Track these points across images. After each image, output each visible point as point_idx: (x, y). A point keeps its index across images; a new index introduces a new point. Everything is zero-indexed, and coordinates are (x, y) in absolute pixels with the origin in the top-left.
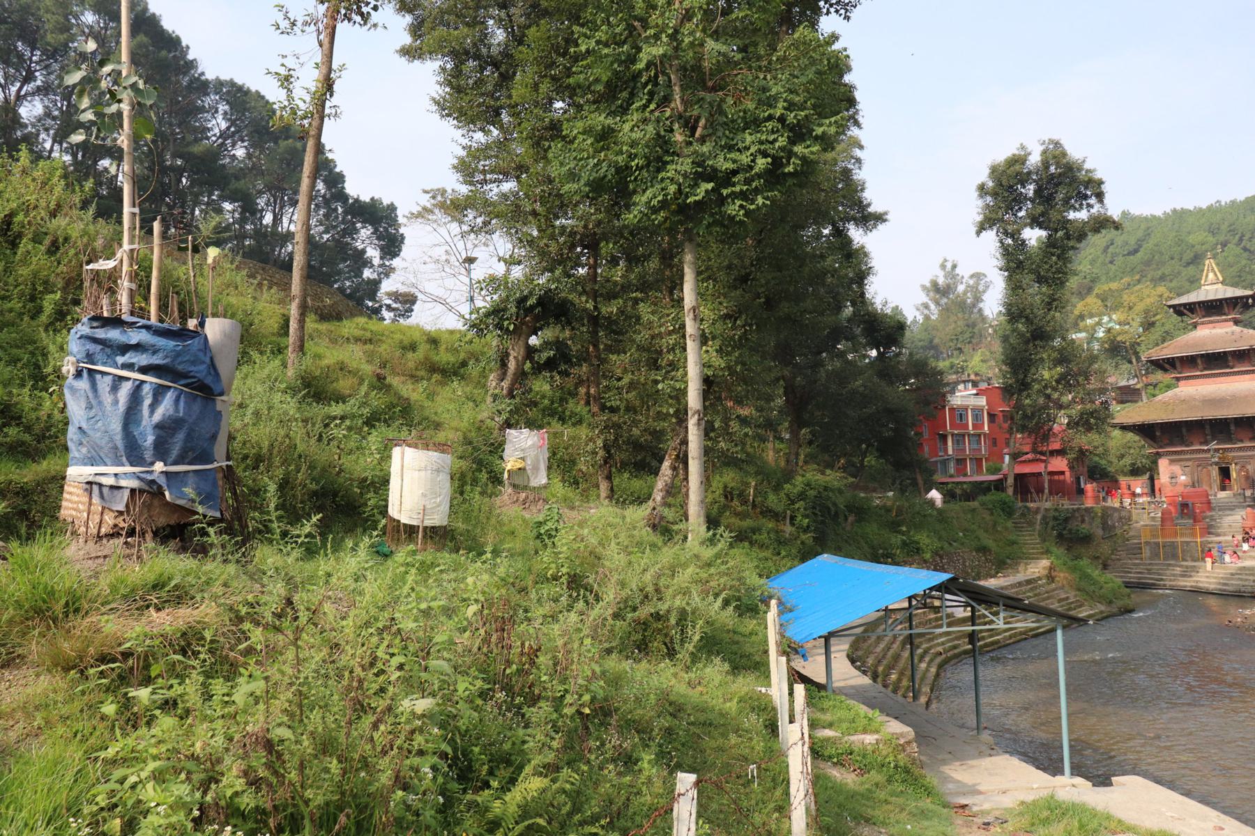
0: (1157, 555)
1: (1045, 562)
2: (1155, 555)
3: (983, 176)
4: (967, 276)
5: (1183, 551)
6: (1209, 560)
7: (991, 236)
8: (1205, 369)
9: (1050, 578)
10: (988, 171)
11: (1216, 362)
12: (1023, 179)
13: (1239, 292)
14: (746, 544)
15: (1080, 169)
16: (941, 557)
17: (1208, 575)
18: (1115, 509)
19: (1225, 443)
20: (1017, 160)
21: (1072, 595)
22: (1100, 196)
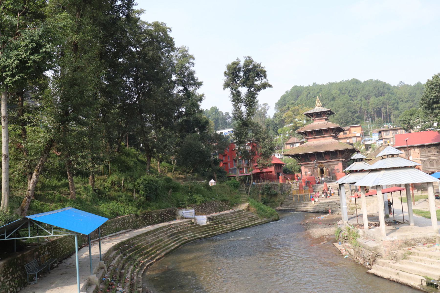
0: (297, 200)
1: (247, 204)
2: (297, 200)
3: (225, 69)
5: (305, 198)
6: (313, 202)
7: (229, 89)
8: (316, 135)
9: (248, 209)
11: (319, 133)
12: (239, 70)
14: (115, 201)
15: (260, 66)
16: (205, 204)
17: (311, 206)
18: (286, 184)
19: (322, 160)
20: (236, 64)
21: (255, 215)
22: (265, 76)
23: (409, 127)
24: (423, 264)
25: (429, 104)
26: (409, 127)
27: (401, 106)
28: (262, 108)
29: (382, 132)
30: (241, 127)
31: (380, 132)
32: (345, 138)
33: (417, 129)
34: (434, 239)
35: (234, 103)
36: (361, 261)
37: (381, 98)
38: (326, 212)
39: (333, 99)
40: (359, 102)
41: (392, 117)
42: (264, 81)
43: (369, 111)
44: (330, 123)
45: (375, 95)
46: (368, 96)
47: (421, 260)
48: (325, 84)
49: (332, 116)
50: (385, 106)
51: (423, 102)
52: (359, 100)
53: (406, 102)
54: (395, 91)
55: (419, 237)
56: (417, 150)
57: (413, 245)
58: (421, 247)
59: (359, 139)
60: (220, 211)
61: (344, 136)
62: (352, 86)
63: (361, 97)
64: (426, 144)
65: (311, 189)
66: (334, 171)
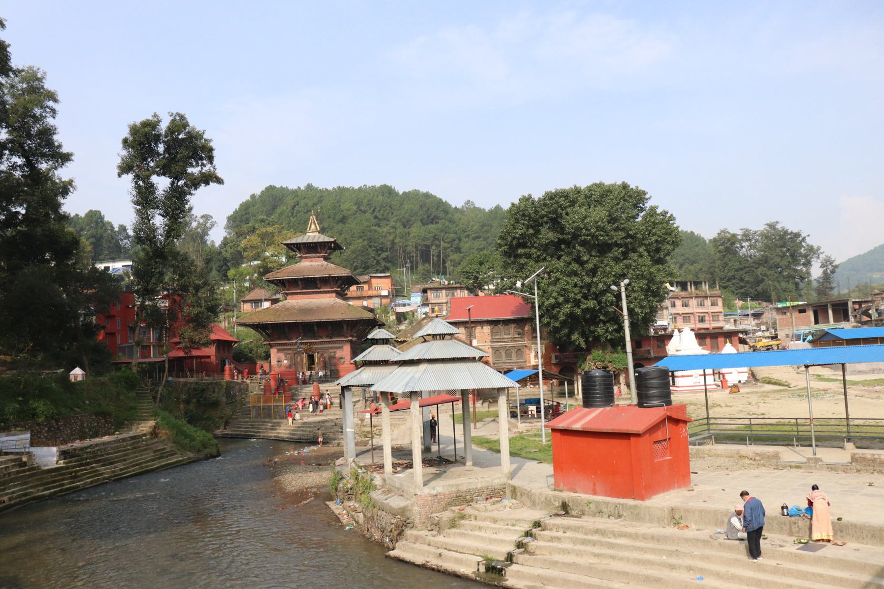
0: (258, 415)
1: (152, 423)
2: (258, 415)
3: (126, 133)
4: (199, 216)
6: (290, 420)
7: (129, 177)
9: (154, 433)
10: (127, 130)
11: (310, 284)
12: (157, 139)
13: (327, 239)
15: (202, 138)
16: (57, 421)
17: (286, 428)
22: (211, 159)
23: (475, 287)
24: (482, 534)
25: (510, 246)
26: (475, 287)
27: (466, 245)
28: (199, 224)
29: (429, 292)
30: (150, 259)
31: (425, 291)
32: (359, 298)
33: (489, 290)
34: (503, 490)
35: (138, 207)
36: (377, 536)
37: (432, 227)
38: (314, 442)
39: (343, 220)
40: (392, 230)
41: (448, 264)
42: (207, 168)
43: (409, 249)
44: (332, 265)
45: (421, 221)
46: (408, 221)
47: (480, 528)
48: (330, 188)
49: (338, 252)
50: (437, 242)
51: (502, 243)
52: (393, 227)
53: (474, 239)
54: (457, 216)
55: (479, 486)
56: (487, 329)
57: (469, 502)
58: (481, 505)
59: (385, 301)
60: (91, 437)
61: (359, 294)
62: (381, 198)
63: (396, 222)
64: (501, 318)
65: (288, 394)
66: (334, 361)
